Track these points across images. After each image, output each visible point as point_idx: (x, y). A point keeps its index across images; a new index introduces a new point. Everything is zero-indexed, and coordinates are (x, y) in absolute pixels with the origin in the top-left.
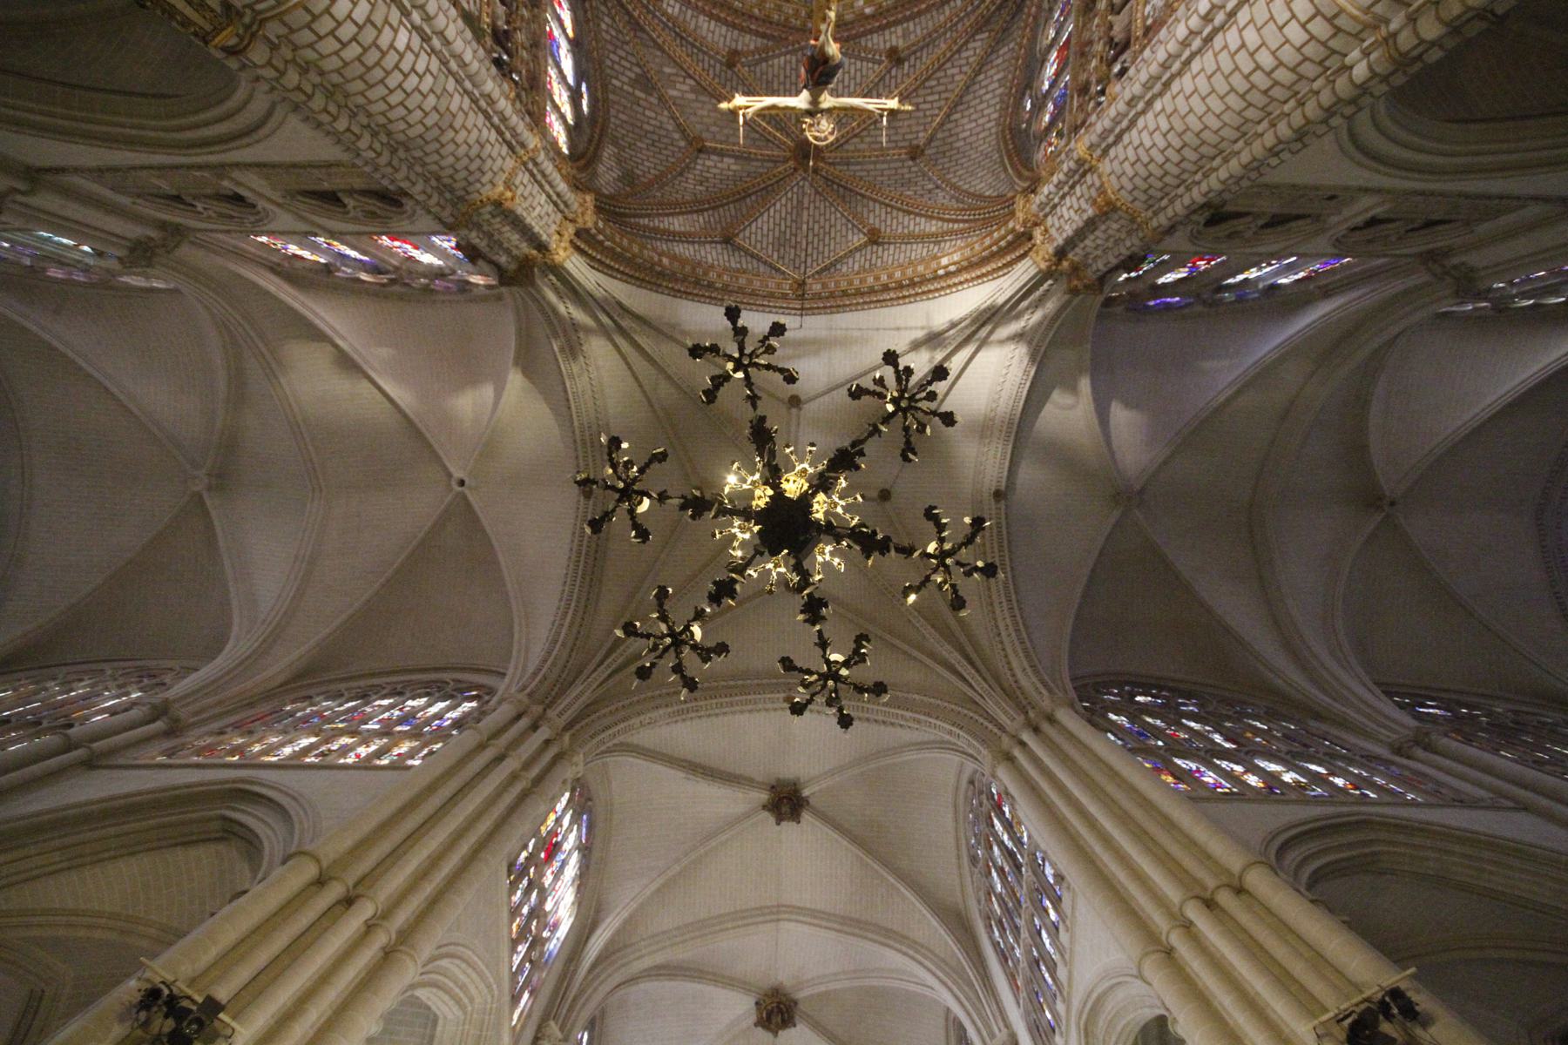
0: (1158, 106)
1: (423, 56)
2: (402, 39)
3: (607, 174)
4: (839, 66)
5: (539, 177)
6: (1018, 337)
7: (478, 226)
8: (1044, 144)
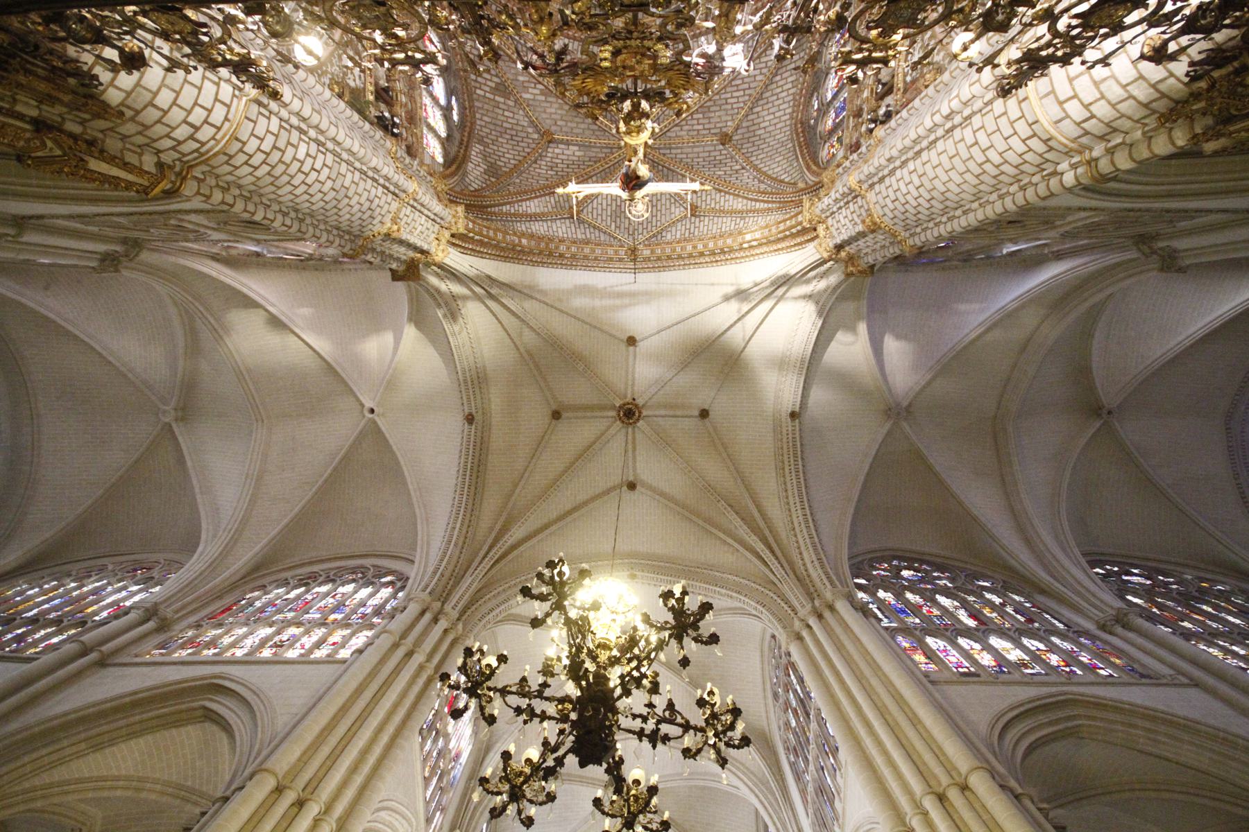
0: (911, 166)
1: (321, 156)
2: (303, 149)
3: (475, 172)
5: (419, 207)
6: (809, 297)
7: (373, 250)
8: (828, 144)
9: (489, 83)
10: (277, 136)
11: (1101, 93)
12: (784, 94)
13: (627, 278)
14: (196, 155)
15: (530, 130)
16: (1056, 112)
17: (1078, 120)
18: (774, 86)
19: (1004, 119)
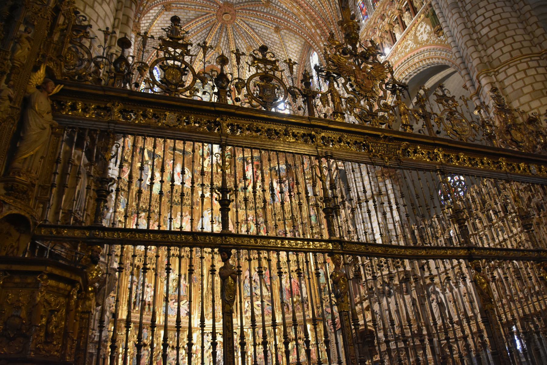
2: (484, 31)
14: (533, 58)
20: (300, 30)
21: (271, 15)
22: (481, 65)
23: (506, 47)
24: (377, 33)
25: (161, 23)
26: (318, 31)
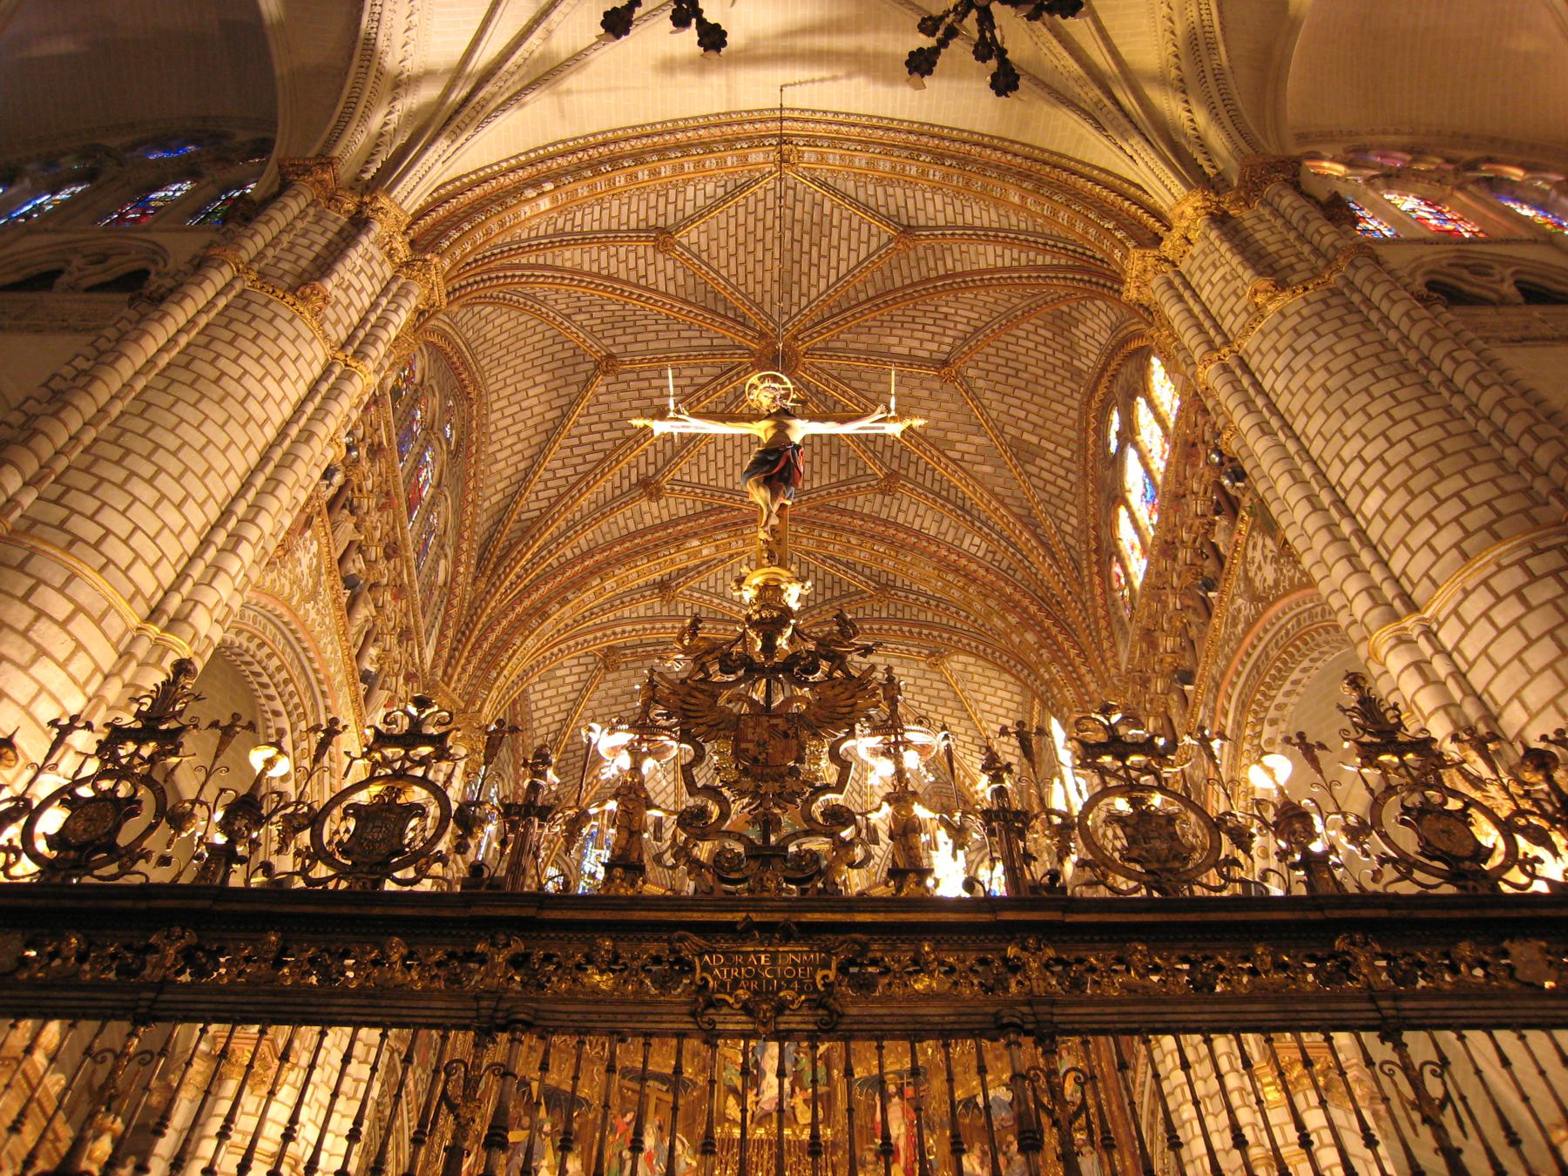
3: (1095, 327)
4: (750, 473)
5: (1207, 324)
6: (400, 84)
7: (1316, 251)
9: (1045, 464)
10: (1403, 541)
11: (30, 640)
12: (509, 441)
13: (799, 98)
15: (981, 383)
16: (82, 593)
17: (42, 588)
18: (527, 453)
19: (152, 559)
20: (987, 645)
21: (902, 622)
22: (1376, 612)
23: (1444, 533)
24: (1171, 600)
25: (601, 705)
26: (1030, 637)
